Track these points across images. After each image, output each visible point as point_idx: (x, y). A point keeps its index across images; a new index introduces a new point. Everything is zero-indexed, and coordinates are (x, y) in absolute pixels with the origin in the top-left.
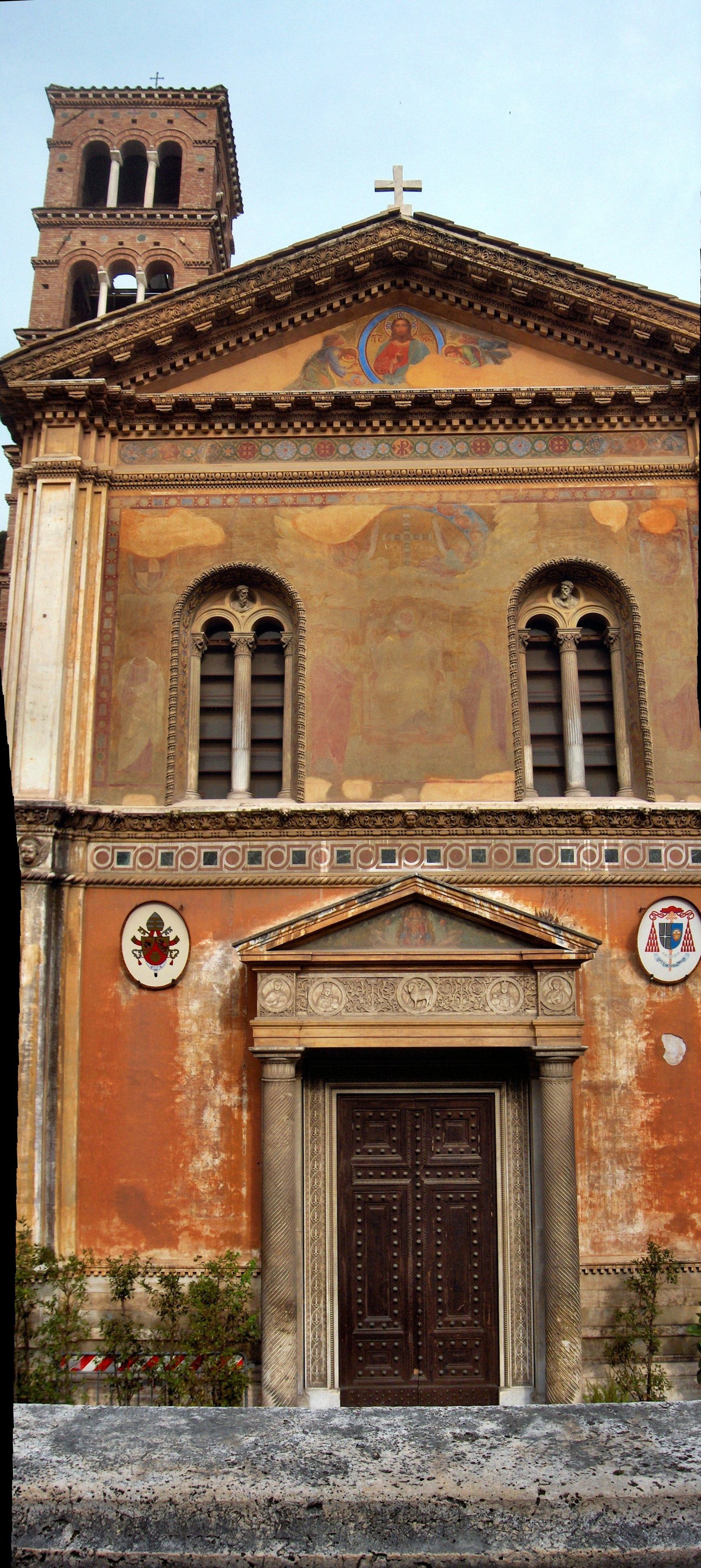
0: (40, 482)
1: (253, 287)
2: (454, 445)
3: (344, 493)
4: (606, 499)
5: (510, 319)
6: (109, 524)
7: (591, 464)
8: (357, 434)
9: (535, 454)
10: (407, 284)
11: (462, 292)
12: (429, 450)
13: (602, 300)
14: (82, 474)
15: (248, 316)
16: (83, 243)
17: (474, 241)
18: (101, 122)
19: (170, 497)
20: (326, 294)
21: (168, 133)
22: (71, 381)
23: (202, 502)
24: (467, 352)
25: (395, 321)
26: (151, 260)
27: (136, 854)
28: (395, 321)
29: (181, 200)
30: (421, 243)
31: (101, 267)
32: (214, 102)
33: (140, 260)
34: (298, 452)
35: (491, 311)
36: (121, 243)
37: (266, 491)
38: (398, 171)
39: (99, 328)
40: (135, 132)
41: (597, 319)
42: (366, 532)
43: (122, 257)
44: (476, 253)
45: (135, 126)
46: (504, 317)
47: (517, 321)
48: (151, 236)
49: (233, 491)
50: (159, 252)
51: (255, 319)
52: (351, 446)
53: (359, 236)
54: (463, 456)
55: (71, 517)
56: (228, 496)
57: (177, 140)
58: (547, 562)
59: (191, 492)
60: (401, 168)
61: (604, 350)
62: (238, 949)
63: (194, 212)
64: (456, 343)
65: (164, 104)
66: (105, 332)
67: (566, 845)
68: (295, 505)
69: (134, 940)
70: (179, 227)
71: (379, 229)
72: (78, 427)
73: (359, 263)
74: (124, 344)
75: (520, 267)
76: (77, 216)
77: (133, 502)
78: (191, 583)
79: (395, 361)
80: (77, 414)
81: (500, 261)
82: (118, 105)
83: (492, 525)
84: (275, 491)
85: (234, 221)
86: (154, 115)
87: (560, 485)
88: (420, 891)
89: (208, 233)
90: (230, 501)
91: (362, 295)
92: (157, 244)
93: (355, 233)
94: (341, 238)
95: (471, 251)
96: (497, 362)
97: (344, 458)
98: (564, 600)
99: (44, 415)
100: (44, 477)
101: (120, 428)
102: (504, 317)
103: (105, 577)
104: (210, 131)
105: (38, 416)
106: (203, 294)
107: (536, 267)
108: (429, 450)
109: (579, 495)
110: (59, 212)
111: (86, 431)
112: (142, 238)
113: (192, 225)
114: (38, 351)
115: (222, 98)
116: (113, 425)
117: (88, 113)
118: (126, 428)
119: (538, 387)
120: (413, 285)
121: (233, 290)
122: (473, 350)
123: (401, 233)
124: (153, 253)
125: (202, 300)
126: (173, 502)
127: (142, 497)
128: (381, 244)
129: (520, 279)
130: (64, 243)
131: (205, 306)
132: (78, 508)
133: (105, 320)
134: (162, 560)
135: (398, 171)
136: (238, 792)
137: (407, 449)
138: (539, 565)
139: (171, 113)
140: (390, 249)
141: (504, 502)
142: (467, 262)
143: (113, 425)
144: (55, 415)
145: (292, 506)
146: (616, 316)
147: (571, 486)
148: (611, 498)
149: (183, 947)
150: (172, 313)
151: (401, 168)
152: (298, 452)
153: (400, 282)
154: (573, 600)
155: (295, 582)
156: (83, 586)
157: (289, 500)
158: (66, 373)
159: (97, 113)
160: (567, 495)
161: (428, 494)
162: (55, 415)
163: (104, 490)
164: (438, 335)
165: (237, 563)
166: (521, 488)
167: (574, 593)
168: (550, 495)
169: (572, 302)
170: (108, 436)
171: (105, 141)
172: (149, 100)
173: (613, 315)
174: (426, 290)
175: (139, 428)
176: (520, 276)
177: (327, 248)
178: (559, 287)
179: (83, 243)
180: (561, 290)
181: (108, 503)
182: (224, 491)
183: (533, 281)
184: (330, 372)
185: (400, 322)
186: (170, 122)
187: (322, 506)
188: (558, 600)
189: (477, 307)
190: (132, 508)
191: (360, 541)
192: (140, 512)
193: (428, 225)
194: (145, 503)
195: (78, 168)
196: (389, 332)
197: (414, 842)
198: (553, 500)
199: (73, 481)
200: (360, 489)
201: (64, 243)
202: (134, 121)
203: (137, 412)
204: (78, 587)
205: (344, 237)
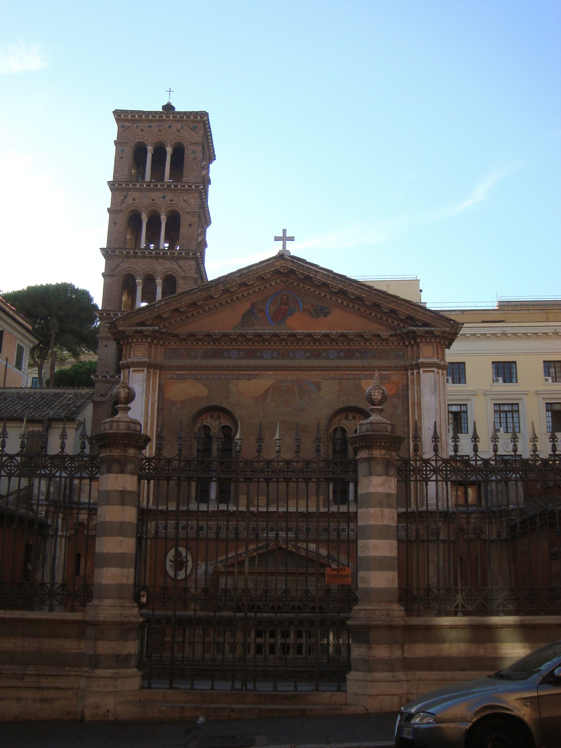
0: (131, 369)
1: (221, 287)
2: (305, 353)
3: (258, 374)
4: (368, 379)
5: (331, 298)
6: (160, 386)
7: (362, 364)
8: (265, 347)
9: (339, 358)
10: (287, 280)
11: (311, 286)
12: (294, 355)
13: (368, 296)
14: (149, 366)
15: (219, 297)
16: (134, 200)
17: (315, 269)
18: (142, 130)
19: (185, 374)
20: (252, 286)
21: (177, 138)
22: (145, 328)
23: (199, 377)
24: (312, 311)
25: (282, 296)
26: (169, 209)
27: (171, 526)
28: (282, 296)
29: (184, 176)
30: (293, 268)
31: (144, 214)
32: (201, 120)
33: (163, 210)
34: (239, 355)
35: (323, 295)
36: (153, 200)
37: (225, 373)
38: (284, 231)
39: (156, 305)
40: (160, 137)
41: (366, 302)
42: (266, 392)
43: (154, 208)
44: (316, 273)
45: (160, 133)
46: (328, 297)
47: (334, 299)
48: (169, 196)
49: (212, 372)
50: (173, 205)
51: (222, 298)
52: (262, 353)
53: (267, 265)
54: (308, 358)
55: (145, 386)
56: (210, 374)
57: (182, 142)
58: (341, 406)
59: (194, 372)
60: (285, 230)
61: (371, 313)
62: (212, 566)
63: (191, 184)
64: (308, 307)
65: (175, 121)
66: (159, 306)
67: (343, 526)
68: (238, 379)
69: (171, 561)
70: (183, 191)
71: (275, 262)
72: (147, 345)
73: (266, 275)
74: (167, 311)
75: (334, 280)
76: (131, 185)
77: (170, 376)
78: (194, 412)
79: (281, 315)
80: (147, 340)
81: (326, 277)
82: (151, 121)
83: (319, 389)
84: (229, 373)
85: (211, 165)
86: (170, 127)
87: (349, 373)
88: (281, 546)
89: (198, 195)
90: (210, 376)
91: (268, 286)
92: (172, 200)
93: (265, 264)
94: (259, 266)
95: (314, 272)
96: (325, 316)
97: (259, 358)
98: (349, 421)
99: (133, 340)
100: (133, 367)
101: (164, 343)
102: (328, 297)
103: (158, 409)
104: (199, 137)
105: (130, 340)
106: (200, 291)
107: (341, 281)
108: (294, 355)
109: (357, 377)
110: (121, 183)
111: (150, 346)
112: (164, 197)
113: (190, 190)
114: (131, 315)
115: (206, 118)
116: (161, 343)
117: (135, 125)
118: (167, 343)
119: (340, 332)
120: (290, 281)
121: (213, 289)
122: (315, 310)
123: (284, 263)
124: (170, 206)
125: (199, 293)
126: (186, 377)
127: (174, 374)
128: (276, 268)
129: (334, 285)
130: (124, 200)
131: (201, 295)
132: (148, 380)
133: (160, 301)
134: (182, 402)
135: (284, 231)
136: (213, 500)
137: (286, 355)
138: (338, 408)
139: (178, 125)
140: (280, 269)
141: (325, 379)
142: (312, 277)
143: (161, 343)
144: (137, 340)
145: (236, 379)
146: (374, 303)
147: (353, 373)
148: (370, 379)
149: (190, 564)
150: (187, 298)
151: (285, 230)
152: (239, 355)
153: (284, 280)
154: (353, 421)
155: (237, 412)
156: (149, 414)
157: (235, 377)
158: (143, 324)
159: (140, 125)
160: (351, 377)
161: (292, 376)
162: (137, 340)
163: (158, 372)
164: (300, 303)
165: (213, 404)
166: (332, 373)
167: (354, 417)
168: (345, 377)
169: (356, 295)
170: (159, 347)
171: (144, 141)
172: (167, 119)
173: (373, 302)
174: (295, 284)
175: (172, 344)
176: (334, 284)
177: (253, 270)
178: (349, 290)
179: (134, 200)
180: (352, 291)
181: (160, 377)
182: (208, 372)
183: (340, 286)
184: (253, 319)
185: (284, 297)
186: (179, 130)
187: (249, 379)
188: (347, 421)
189: (317, 293)
190: (170, 379)
191: (265, 395)
192: (173, 381)
193: (296, 261)
194: (175, 377)
195: (131, 157)
196: (279, 301)
197: (282, 524)
198: (344, 379)
199: (146, 369)
200: (265, 372)
201: (124, 200)
202: (160, 130)
203: (172, 337)
204: (148, 414)
205: (260, 265)
